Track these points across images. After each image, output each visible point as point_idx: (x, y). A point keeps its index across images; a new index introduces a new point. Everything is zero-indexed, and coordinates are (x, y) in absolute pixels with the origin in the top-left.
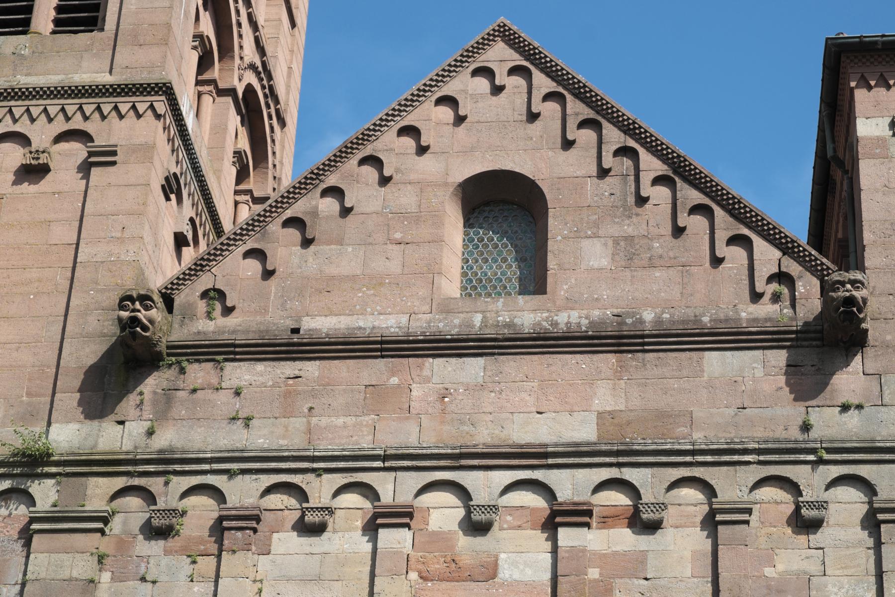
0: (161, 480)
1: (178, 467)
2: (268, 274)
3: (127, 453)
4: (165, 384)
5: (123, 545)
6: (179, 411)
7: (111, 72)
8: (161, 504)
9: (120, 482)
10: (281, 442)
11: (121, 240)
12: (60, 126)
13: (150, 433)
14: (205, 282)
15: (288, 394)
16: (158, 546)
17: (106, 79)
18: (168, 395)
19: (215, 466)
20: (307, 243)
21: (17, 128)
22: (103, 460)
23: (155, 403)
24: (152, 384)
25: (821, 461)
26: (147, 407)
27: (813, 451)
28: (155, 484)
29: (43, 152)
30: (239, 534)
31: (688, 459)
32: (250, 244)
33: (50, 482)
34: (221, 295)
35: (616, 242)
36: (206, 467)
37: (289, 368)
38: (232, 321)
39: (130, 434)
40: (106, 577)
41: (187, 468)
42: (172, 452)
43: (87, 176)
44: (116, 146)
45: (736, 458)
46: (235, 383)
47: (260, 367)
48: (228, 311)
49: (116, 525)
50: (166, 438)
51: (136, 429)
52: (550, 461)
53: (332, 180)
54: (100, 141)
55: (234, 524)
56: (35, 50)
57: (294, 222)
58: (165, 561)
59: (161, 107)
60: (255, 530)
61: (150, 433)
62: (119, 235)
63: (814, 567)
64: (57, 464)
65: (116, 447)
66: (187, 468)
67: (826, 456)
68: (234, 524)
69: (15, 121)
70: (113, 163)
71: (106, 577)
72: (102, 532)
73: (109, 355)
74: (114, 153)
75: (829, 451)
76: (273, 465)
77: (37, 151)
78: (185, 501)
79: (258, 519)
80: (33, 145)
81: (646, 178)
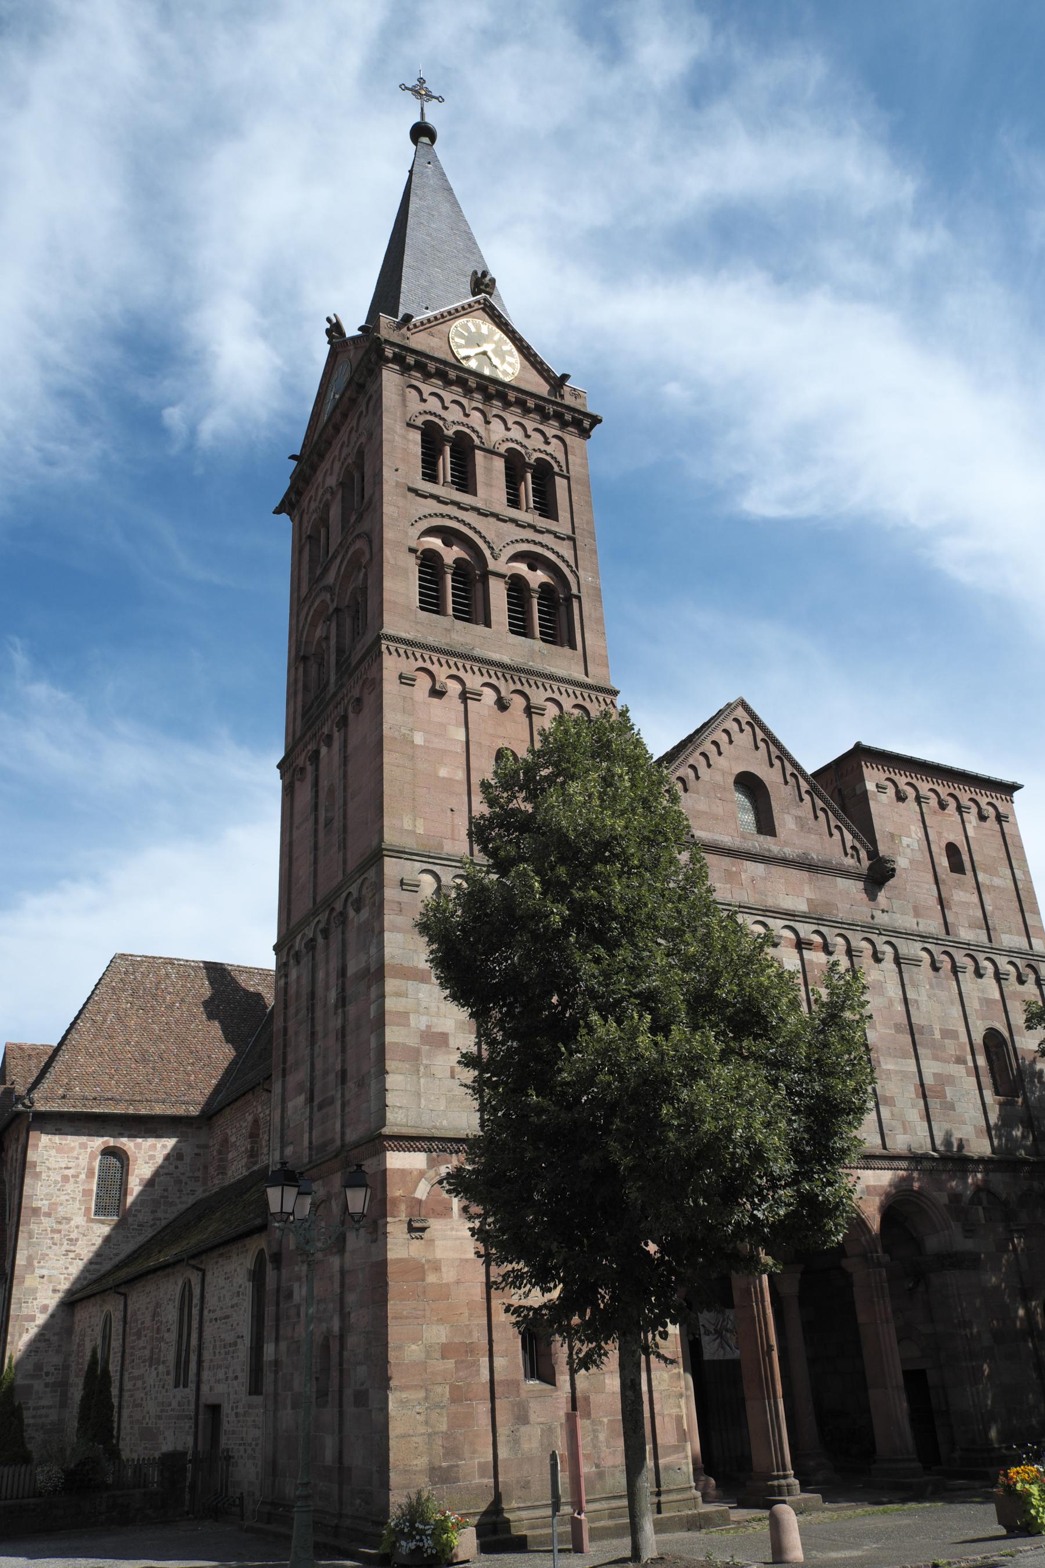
7: (587, 674)
25: (880, 934)
27: (878, 929)
31: (840, 925)
35: (796, 818)
45: (854, 928)
52: (797, 918)
63: (882, 979)
67: (883, 932)
75: (885, 930)
81: (803, 790)
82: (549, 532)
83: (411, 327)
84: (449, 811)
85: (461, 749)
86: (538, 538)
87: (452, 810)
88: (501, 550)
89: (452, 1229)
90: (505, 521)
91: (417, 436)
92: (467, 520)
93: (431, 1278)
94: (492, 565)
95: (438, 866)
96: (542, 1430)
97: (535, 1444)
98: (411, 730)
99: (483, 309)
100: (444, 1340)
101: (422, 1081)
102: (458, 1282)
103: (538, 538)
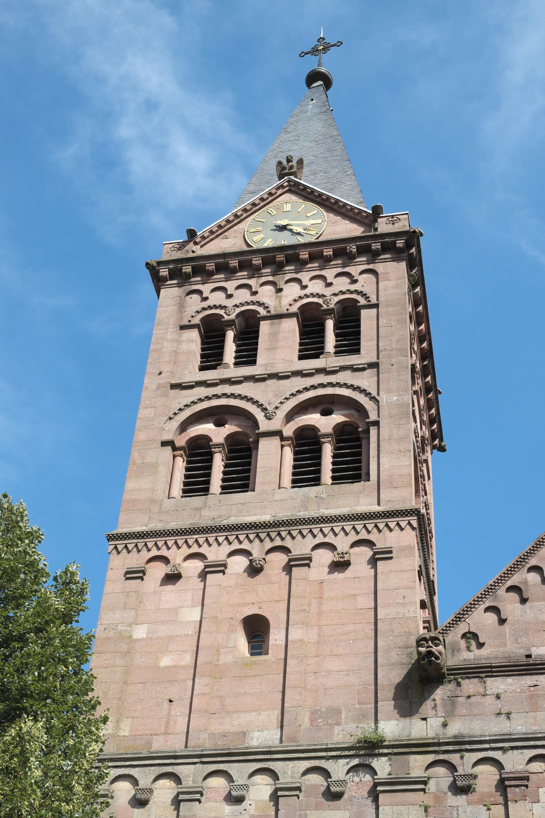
0: (458, 755)
1: (468, 747)
2: (502, 621)
3: (433, 738)
4: (449, 693)
5: (439, 799)
6: (461, 710)
7: (379, 504)
8: (460, 771)
9: (431, 758)
10: (534, 728)
11: (404, 605)
12: (353, 537)
13: (445, 725)
14: (462, 628)
15: (531, 697)
16: (461, 800)
17: (376, 508)
18: (452, 699)
19: (493, 745)
20: (524, 601)
21: (327, 540)
22: (418, 744)
23: (444, 705)
26: (439, 708)
28: (454, 758)
29: (346, 553)
30: (517, 790)
32: (488, 603)
33: (385, 759)
34: (475, 636)
36: (487, 746)
37: (529, 680)
38: (484, 652)
39: (431, 726)
41: (475, 747)
42: (463, 737)
43: (375, 567)
44: (391, 548)
46: (496, 691)
47: (510, 680)
48: (480, 645)
49: (432, 786)
53: (533, 562)
54: (380, 545)
55: (513, 783)
56: (329, 494)
57: (511, 589)
58: (469, 809)
59: (415, 524)
60: (527, 786)
61: (445, 725)
62: (402, 601)
64: (388, 747)
65: (424, 734)
66: (475, 747)
68: (513, 783)
69: (325, 536)
70: (391, 558)
72: (423, 790)
73: (408, 676)
74: (391, 552)
76: (532, 743)
77: (342, 553)
78: (475, 768)
79: (527, 779)
80: (338, 550)
82: (343, 368)
83: (198, 240)
84: (166, 703)
85: (192, 631)
86: (332, 379)
87: (171, 701)
88: (277, 408)
90: (287, 377)
91: (194, 335)
92: (243, 393)
94: (264, 425)
95: (137, 769)
98: (130, 625)
99: (289, 191)
103: (332, 379)
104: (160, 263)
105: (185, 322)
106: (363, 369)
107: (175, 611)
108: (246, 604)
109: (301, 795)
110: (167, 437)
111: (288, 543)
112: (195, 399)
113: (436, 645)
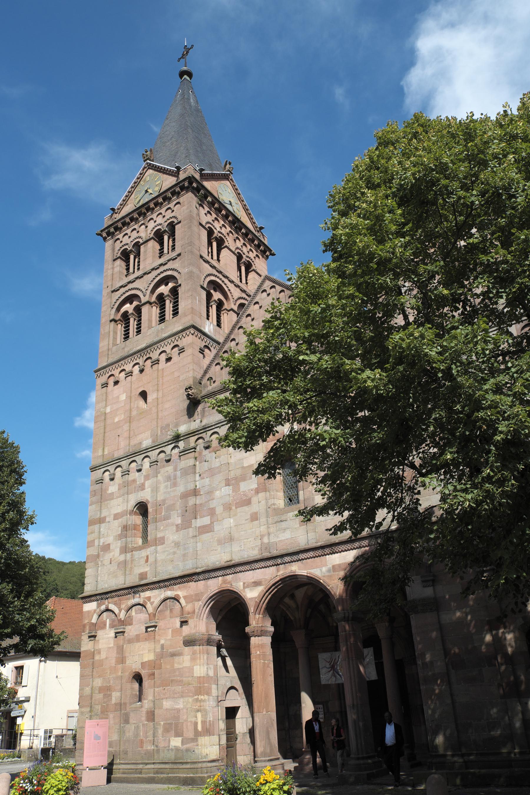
0: (205, 433)
1: (208, 429)
4: (202, 407)
5: (200, 453)
6: (206, 414)
9: (196, 437)
12: (172, 345)
13: (201, 421)
14: (208, 376)
23: (201, 413)
24: (200, 408)
26: (199, 415)
28: (203, 435)
32: (216, 362)
33: (182, 441)
36: (214, 427)
40: (198, 463)
41: (210, 429)
48: (214, 382)
49: (198, 449)
50: (205, 422)
51: (198, 421)
53: (232, 337)
58: (209, 455)
61: (201, 421)
64: (183, 436)
66: (210, 429)
71: (198, 463)
74: (184, 348)
82: (169, 261)
89: (106, 634)
90: (150, 272)
93: (97, 657)
96: (135, 727)
97: (131, 734)
100: (100, 685)
101: (100, 568)
102: (107, 658)
104: (102, 231)
105: (115, 258)
106: (176, 258)
107: (118, 397)
108: (139, 387)
109: (158, 464)
110: (112, 318)
111: (151, 355)
112: (119, 296)
113: (191, 390)
